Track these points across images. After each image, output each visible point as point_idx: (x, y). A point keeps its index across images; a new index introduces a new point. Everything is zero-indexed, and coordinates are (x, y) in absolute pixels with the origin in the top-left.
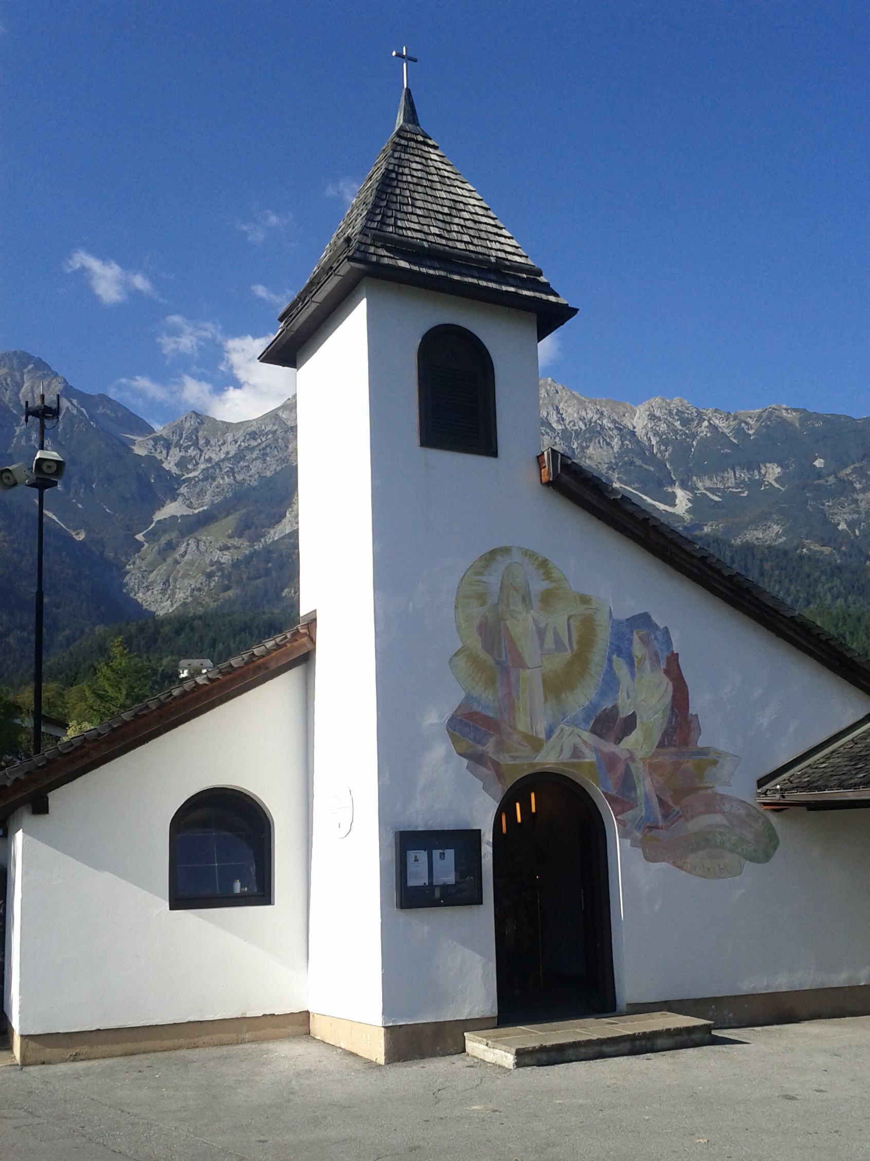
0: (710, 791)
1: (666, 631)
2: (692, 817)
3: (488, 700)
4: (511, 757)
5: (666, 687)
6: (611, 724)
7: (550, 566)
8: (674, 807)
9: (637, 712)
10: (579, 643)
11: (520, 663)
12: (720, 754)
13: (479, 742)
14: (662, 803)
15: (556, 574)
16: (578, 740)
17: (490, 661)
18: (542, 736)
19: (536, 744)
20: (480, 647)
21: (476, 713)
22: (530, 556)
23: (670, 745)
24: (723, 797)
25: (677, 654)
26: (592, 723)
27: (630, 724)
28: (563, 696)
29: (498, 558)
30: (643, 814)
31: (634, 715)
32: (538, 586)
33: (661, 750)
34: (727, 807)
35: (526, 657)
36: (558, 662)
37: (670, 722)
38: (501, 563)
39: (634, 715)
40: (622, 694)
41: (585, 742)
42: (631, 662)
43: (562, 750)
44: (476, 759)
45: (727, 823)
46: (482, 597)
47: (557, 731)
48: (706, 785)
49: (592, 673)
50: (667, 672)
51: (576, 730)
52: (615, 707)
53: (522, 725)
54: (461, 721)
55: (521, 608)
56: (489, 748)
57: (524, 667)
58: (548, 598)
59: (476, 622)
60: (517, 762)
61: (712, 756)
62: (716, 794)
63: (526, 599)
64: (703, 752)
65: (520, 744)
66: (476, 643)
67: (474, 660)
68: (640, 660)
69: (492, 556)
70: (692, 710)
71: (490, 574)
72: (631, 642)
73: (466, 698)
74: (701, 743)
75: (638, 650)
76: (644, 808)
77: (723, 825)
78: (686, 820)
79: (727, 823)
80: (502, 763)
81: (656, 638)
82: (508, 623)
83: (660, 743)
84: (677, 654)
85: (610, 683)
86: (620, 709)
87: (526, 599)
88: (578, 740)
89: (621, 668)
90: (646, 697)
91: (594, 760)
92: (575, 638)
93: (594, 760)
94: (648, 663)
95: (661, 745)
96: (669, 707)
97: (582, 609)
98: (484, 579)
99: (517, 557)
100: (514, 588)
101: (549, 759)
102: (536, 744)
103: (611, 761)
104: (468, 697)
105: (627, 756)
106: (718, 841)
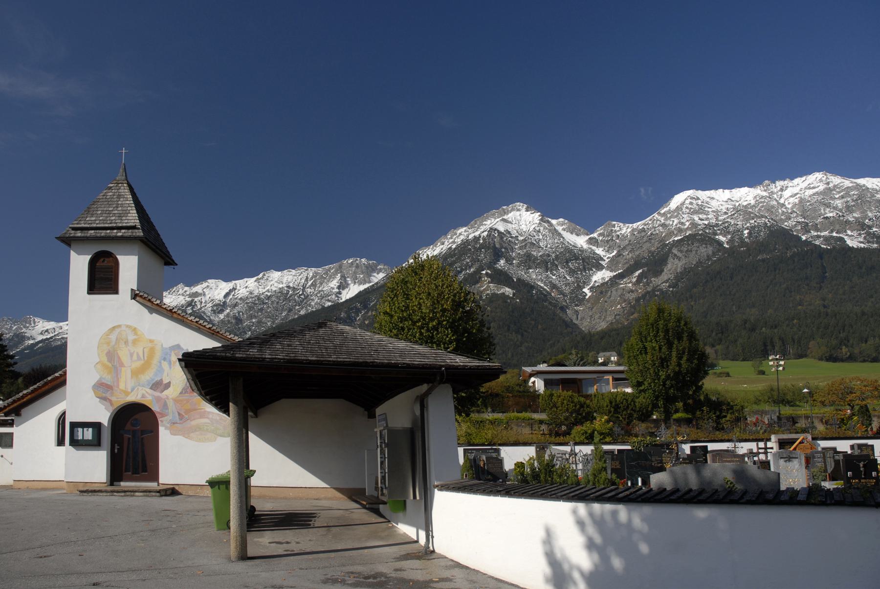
3: (108, 379)
6: (159, 386)
11: (122, 365)
14: (179, 414)
17: (110, 365)
19: (127, 394)
27: (168, 385)
31: (169, 383)
32: (131, 337)
34: (210, 416)
36: (138, 364)
38: (117, 330)
39: (169, 383)
40: (165, 374)
42: (170, 363)
44: (103, 399)
46: (108, 344)
53: (122, 386)
56: (108, 395)
58: (135, 342)
63: (126, 343)
66: (105, 359)
67: (104, 365)
69: (114, 328)
85: (160, 370)
87: (126, 343)
89: (165, 365)
97: (150, 345)
99: (123, 328)
101: (132, 398)
102: (127, 394)
103: (158, 399)
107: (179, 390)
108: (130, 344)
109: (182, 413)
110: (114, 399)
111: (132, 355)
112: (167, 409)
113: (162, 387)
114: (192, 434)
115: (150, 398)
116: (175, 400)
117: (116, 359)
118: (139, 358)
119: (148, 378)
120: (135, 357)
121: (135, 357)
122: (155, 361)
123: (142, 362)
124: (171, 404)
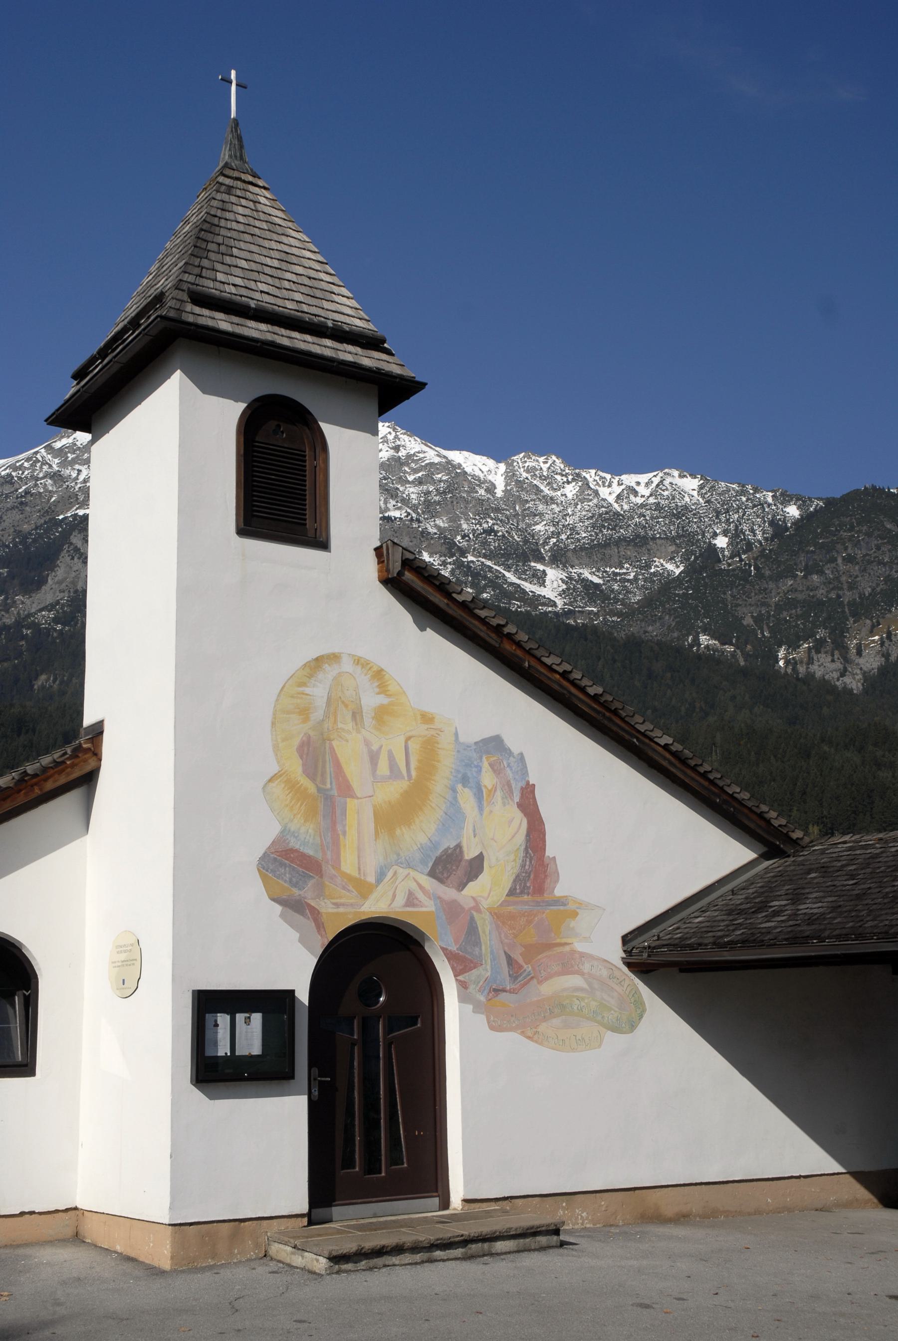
0: (567, 948)
1: (521, 758)
2: (546, 979)
3: (307, 837)
4: (334, 904)
5: (520, 822)
6: (454, 867)
7: (387, 677)
8: (525, 966)
9: (485, 854)
10: (418, 769)
11: (347, 790)
12: (580, 904)
13: (295, 885)
14: (510, 961)
15: (392, 688)
16: (413, 886)
17: (311, 788)
18: (371, 879)
20: (300, 770)
21: (292, 850)
22: (363, 666)
23: (522, 892)
24: (582, 955)
25: (534, 785)
26: (430, 864)
27: (476, 866)
28: (398, 832)
29: (326, 666)
30: (489, 974)
31: (480, 858)
33: (511, 898)
34: (586, 968)
35: (355, 784)
37: (523, 866)
38: (329, 672)
39: (480, 858)
40: (468, 831)
41: (421, 887)
43: (394, 896)
44: (294, 906)
45: (586, 986)
46: (304, 712)
47: (390, 874)
48: (564, 940)
49: (433, 805)
50: (519, 805)
51: (413, 873)
52: (459, 846)
53: (349, 865)
54: (275, 859)
55: (350, 726)
56: (307, 893)
57: (353, 796)
58: (382, 715)
59: (296, 742)
60: (341, 910)
61: (571, 906)
62: (573, 952)
64: (561, 902)
65: (344, 888)
66: (295, 767)
67: (292, 786)
68: (490, 791)
69: (318, 663)
70: (549, 853)
71: (314, 686)
72: (479, 769)
73: (282, 832)
74: (559, 892)
75: (488, 779)
76: (489, 967)
77: (582, 989)
78: (540, 982)
79: (586, 986)
80: (323, 910)
81: (509, 765)
82: (334, 743)
83: (510, 890)
84: (534, 785)
85: (453, 817)
86: (465, 849)
87: (357, 715)
88: (413, 886)
89: (466, 799)
90: (495, 834)
91: (433, 909)
92: (413, 764)
93: (433, 909)
94: (499, 794)
95: (512, 893)
96: (523, 847)
97: (422, 730)
98: (307, 690)
99: (347, 666)
100: (343, 702)
101: (377, 905)
102: (364, 889)
103: (452, 910)
104: (284, 831)
105: (472, 904)
106: (575, 1008)
107: (507, 883)
108: (368, 720)
109: (517, 956)
110: (326, 907)
111: (374, 758)
112: (477, 943)
113: (460, 872)
114: (543, 1027)
115: (429, 906)
116: (498, 915)
117: (329, 768)
118: (394, 772)
119: (422, 839)
120: (383, 767)
121: (383, 767)
122: (439, 785)
123: (403, 785)
124: (485, 925)
